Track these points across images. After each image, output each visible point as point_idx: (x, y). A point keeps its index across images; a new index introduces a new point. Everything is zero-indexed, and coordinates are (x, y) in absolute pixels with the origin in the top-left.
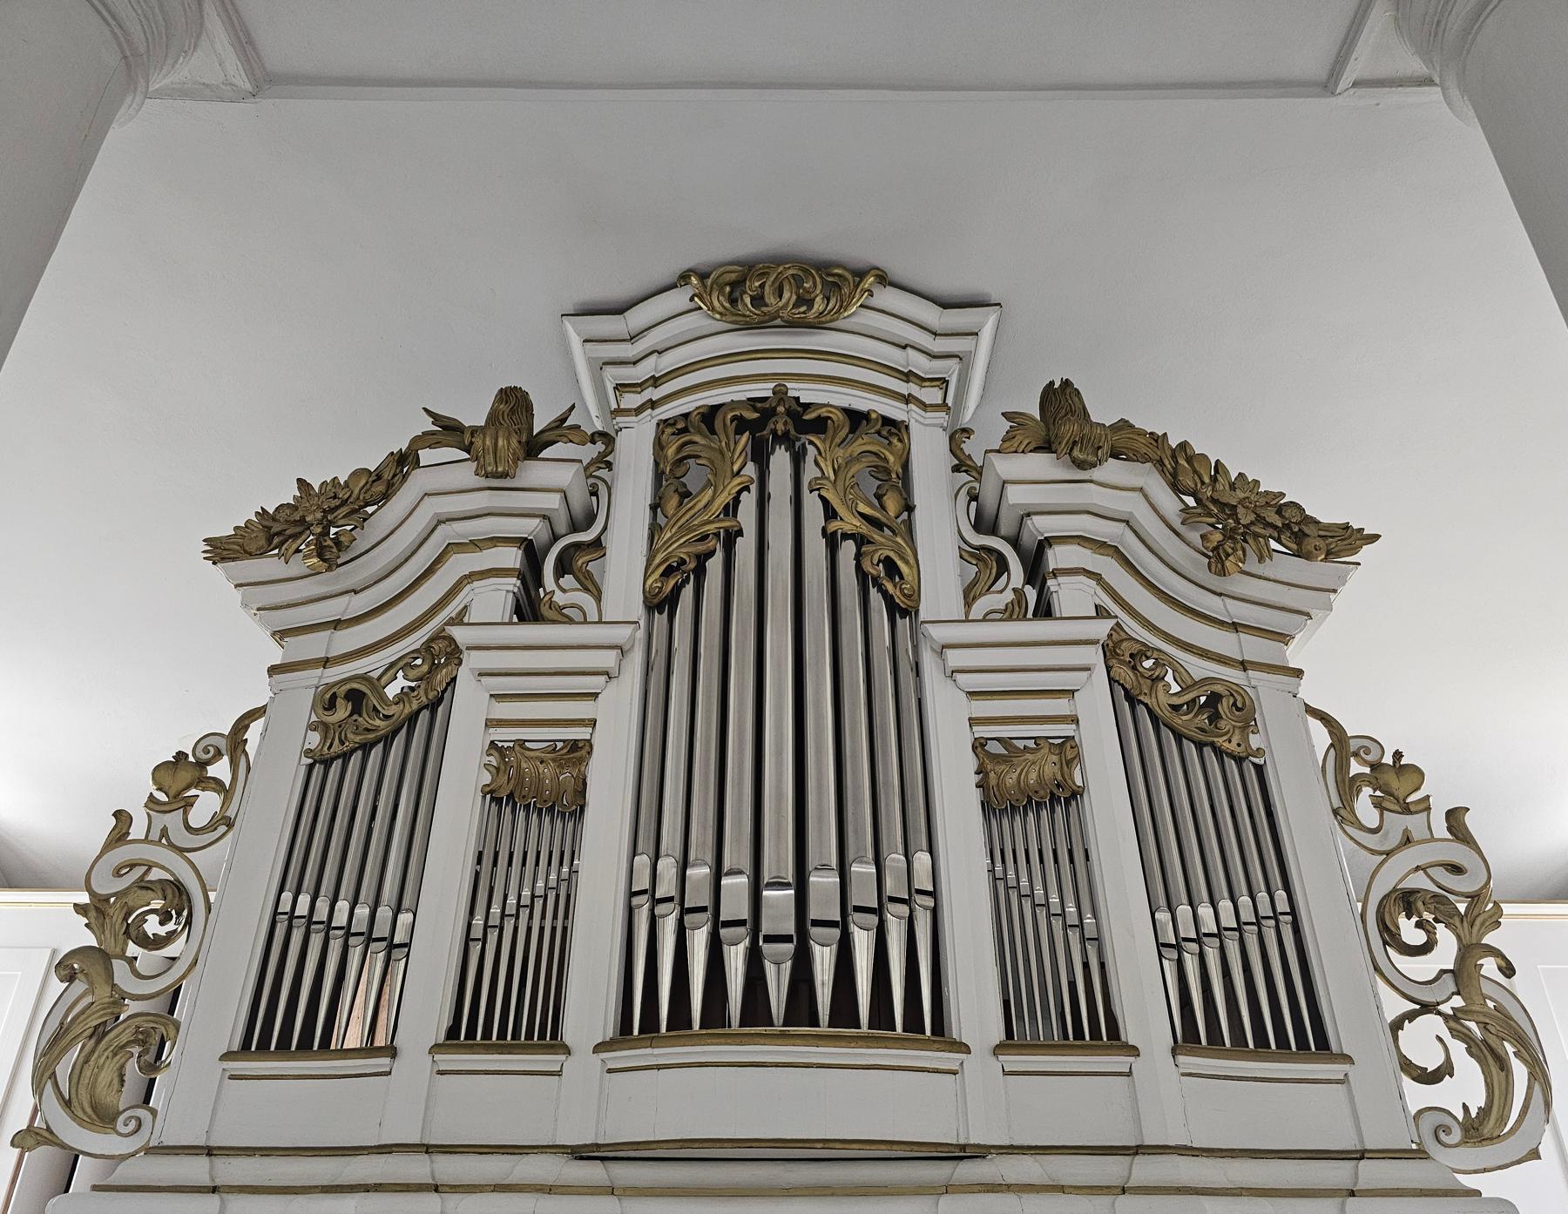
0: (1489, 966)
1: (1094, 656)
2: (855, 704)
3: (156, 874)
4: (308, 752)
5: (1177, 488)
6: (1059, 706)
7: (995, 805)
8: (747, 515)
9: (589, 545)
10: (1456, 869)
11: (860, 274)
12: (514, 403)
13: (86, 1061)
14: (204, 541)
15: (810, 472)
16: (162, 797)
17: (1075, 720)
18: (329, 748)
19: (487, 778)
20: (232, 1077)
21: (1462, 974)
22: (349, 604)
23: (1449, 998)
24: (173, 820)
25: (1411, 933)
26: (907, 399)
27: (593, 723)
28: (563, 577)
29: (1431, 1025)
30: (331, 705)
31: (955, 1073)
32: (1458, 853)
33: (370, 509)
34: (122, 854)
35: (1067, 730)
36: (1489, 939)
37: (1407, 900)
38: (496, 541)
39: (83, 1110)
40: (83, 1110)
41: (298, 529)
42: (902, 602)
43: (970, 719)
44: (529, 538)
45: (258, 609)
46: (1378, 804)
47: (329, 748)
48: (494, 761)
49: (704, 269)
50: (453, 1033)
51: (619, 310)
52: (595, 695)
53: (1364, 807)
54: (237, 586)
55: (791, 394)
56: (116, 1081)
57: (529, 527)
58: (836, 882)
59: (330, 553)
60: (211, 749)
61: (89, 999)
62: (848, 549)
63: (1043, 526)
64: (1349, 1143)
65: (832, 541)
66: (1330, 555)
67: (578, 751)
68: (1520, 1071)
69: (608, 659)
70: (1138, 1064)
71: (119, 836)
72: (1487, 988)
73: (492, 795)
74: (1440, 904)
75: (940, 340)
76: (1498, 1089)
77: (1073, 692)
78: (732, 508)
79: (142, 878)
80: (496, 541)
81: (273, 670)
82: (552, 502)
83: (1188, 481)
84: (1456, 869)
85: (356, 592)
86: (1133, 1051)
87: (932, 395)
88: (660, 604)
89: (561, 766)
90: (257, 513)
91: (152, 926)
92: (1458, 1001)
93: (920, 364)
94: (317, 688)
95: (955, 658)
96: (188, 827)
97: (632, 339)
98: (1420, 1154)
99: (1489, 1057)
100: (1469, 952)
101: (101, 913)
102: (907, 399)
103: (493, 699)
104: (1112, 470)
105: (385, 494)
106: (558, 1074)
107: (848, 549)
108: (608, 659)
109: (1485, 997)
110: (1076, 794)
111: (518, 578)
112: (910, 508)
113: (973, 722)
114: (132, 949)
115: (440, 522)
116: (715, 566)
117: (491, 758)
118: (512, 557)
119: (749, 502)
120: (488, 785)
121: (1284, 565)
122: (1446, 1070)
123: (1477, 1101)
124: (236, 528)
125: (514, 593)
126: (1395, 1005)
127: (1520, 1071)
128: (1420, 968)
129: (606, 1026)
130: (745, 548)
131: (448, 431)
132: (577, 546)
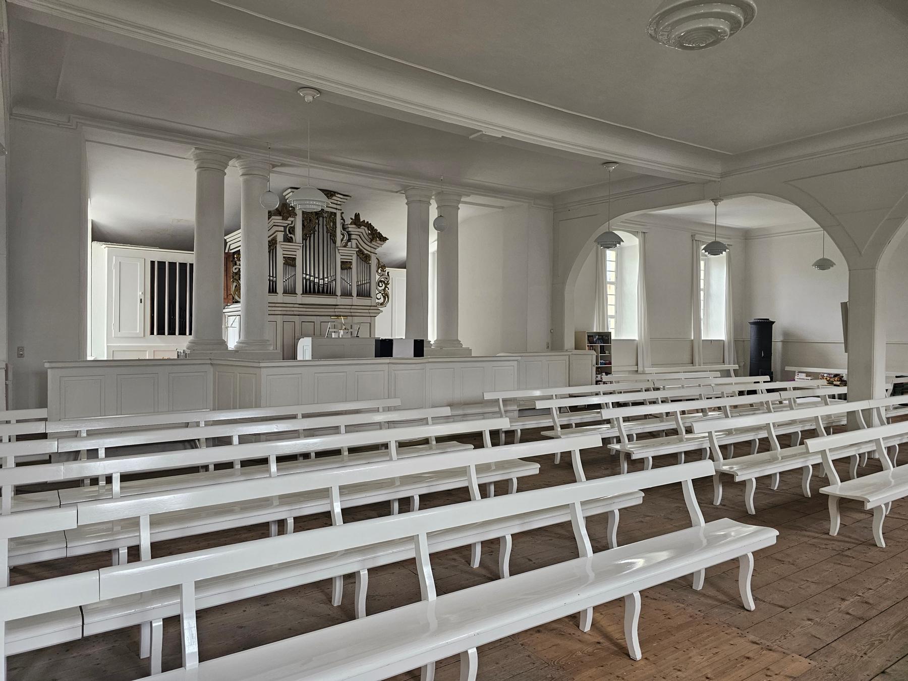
0: (387, 289)
1: (355, 252)
5: (368, 230)
6: (350, 258)
8: (316, 228)
10: (387, 278)
11: (335, 192)
15: (325, 223)
17: (352, 259)
21: (384, 290)
25: (381, 285)
26: (337, 209)
27: (296, 255)
28: (225, 174)
29: (380, 294)
32: (387, 277)
35: (351, 261)
37: (381, 281)
53: (379, 271)
62: (329, 234)
63: (352, 233)
64: (370, 305)
66: (383, 241)
67: (294, 259)
68: (387, 299)
74: (384, 282)
78: (314, 228)
83: (370, 228)
84: (387, 278)
86: (353, 296)
87: (338, 207)
88: (304, 239)
93: (339, 203)
95: (340, 251)
98: (376, 306)
99: (384, 298)
100: (386, 287)
104: (362, 227)
110: (351, 269)
112: (336, 227)
116: (312, 235)
119: (317, 225)
121: (379, 242)
126: (378, 292)
127: (387, 299)
128: (380, 288)
129: (301, 293)
130: (316, 233)
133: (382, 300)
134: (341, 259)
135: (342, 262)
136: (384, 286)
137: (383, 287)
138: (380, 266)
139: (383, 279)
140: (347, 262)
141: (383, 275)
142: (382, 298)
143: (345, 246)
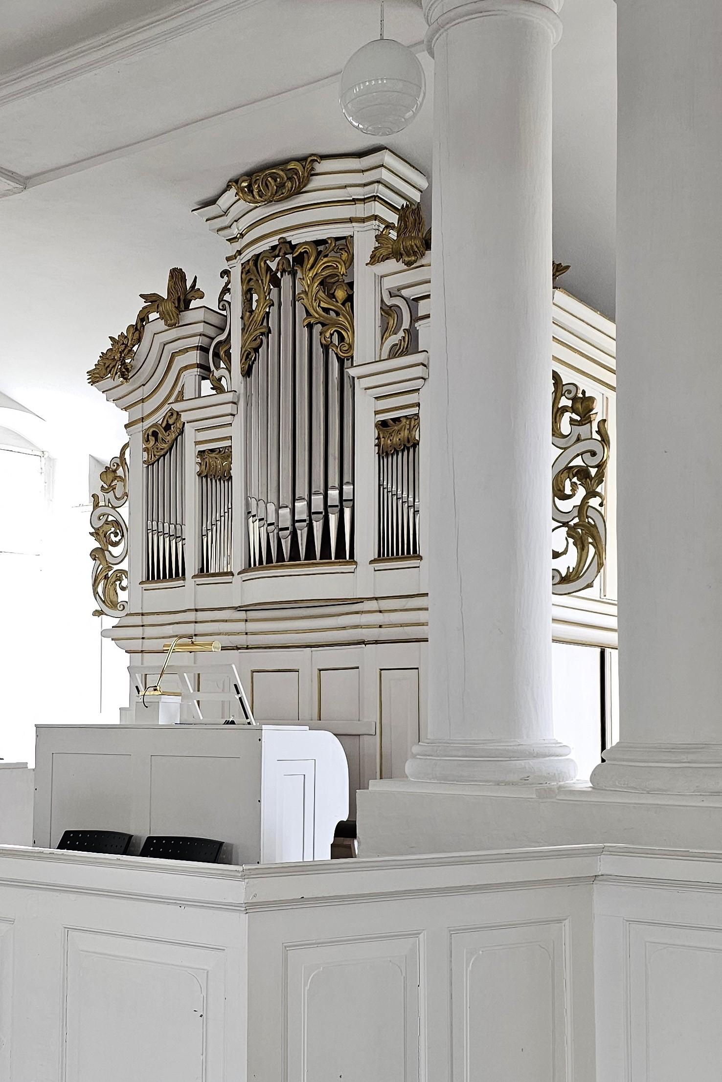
2: (348, 399)
3: (110, 518)
4: (144, 462)
7: (384, 453)
9: (224, 342)
10: (593, 454)
12: (177, 275)
13: (105, 588)
14: (87, 373)
16: (105, 486)
18: (151, 459)
19: (198, 469)
20: (145, 590)
21: (582, 508)
22: (143, 391)
23: (573, 520)
24: (111, 495)
26: (351, 220)
30: (148, 441)
31: (353, 573)
33: (135, 349)
34: (99, 511)
35: (414, 411)
36: (598, 490)
38: (186, 350)
39: (108, 603)
40: (108, 603)
41: (114, 363)
42: (342, 356)
43: (375, 412)
44: (200, 345)
45: (113, 401)
46: (572, 422)
47: (151, 459)
48: (199, 460)
49: (235, 179)
50: (202, 570)
51: (212, 202)
52: (231, 424)
53: (565, 427)
54: (103, 392)
55: (288, 239)
56: (115, 594)
57: (196, 341)
58: (320, 498)
59: (125, 373)
60: (115, 464)
61: (101, 566)
65: (310, 326)
68: (592, 550)
69: (228, 408)
70: (422, 564)
71: (96, 505)
72: (590, 512)
73: (199, 474)
75: (366, 173)
76: (581, 559)
77: (419, 389)
79: (106, 520)
80: (186, 350)
81: (126, 426)
82: (200, 328)
85: (144, 385)
89: (222, 459)
90: (100, 356)
91: (114, 539)
92: (576, 520)
93: (358, 193)
94: (143, 431)
96: (116, 498)
97: (225, 213)
101: (97, 534)
102: (351, 220)
103: (197, 431)
105: (138, 339)
106: (231, 583)
107: (318, 328)
108: (228, 408)
109: (588, 517)
110: (416, 444)
111: (198, 368)
113: (377, 413)
114: (110, 548)
115: (165, 345)
117: (199, 459)
118: (194, 357)
120: (198, 472)
122: (565, 552)
123: (573, 564)
124: (95, 365)
125: (199, 375)
127: (592, 550)
128: (565, 506)
131: (152, 300)
132: (220, 343)
133: (569, 561)
134: (377, 413)
135: (383, 425)
136: (581, 492)
137: (577, 500)
138: (565, 402)
139: (578, 462)
140: (396, 420)
141: (578, 440)
142: (573, 551)
143: (396, 352)
